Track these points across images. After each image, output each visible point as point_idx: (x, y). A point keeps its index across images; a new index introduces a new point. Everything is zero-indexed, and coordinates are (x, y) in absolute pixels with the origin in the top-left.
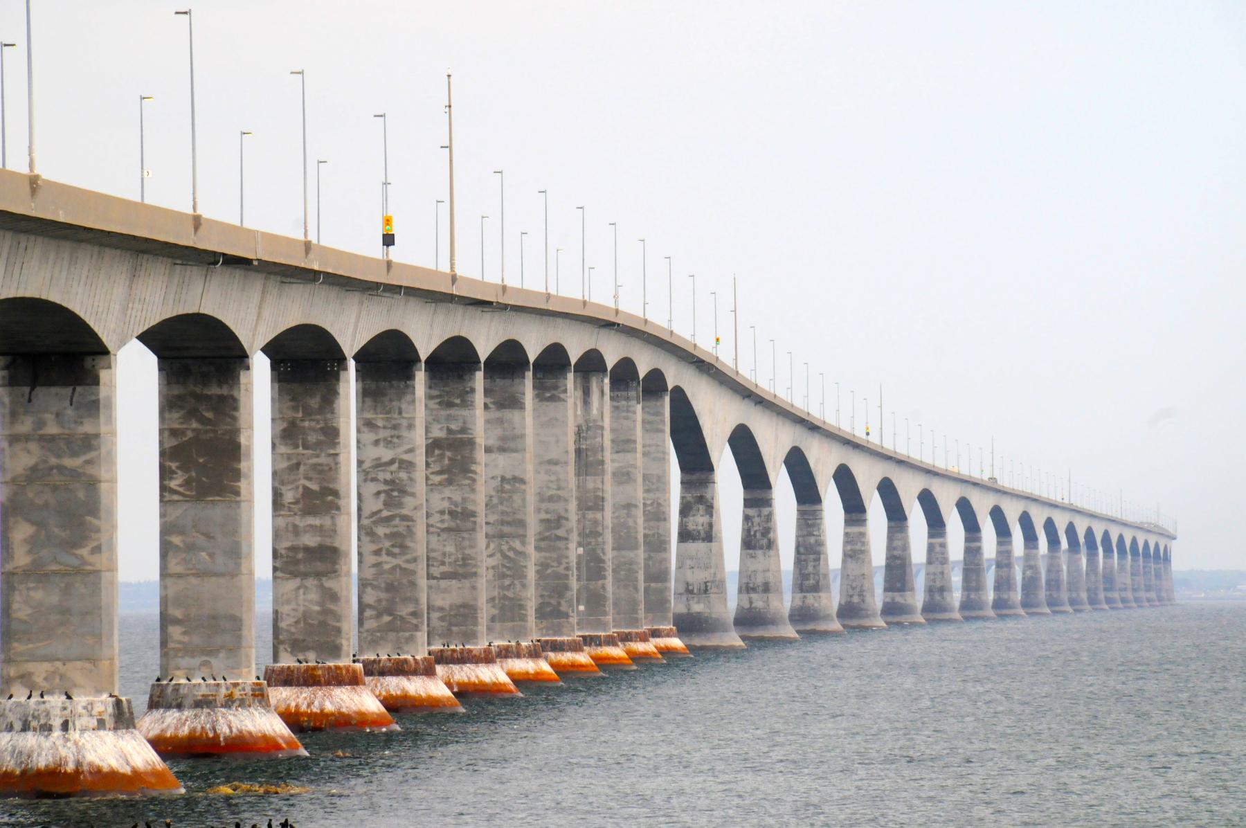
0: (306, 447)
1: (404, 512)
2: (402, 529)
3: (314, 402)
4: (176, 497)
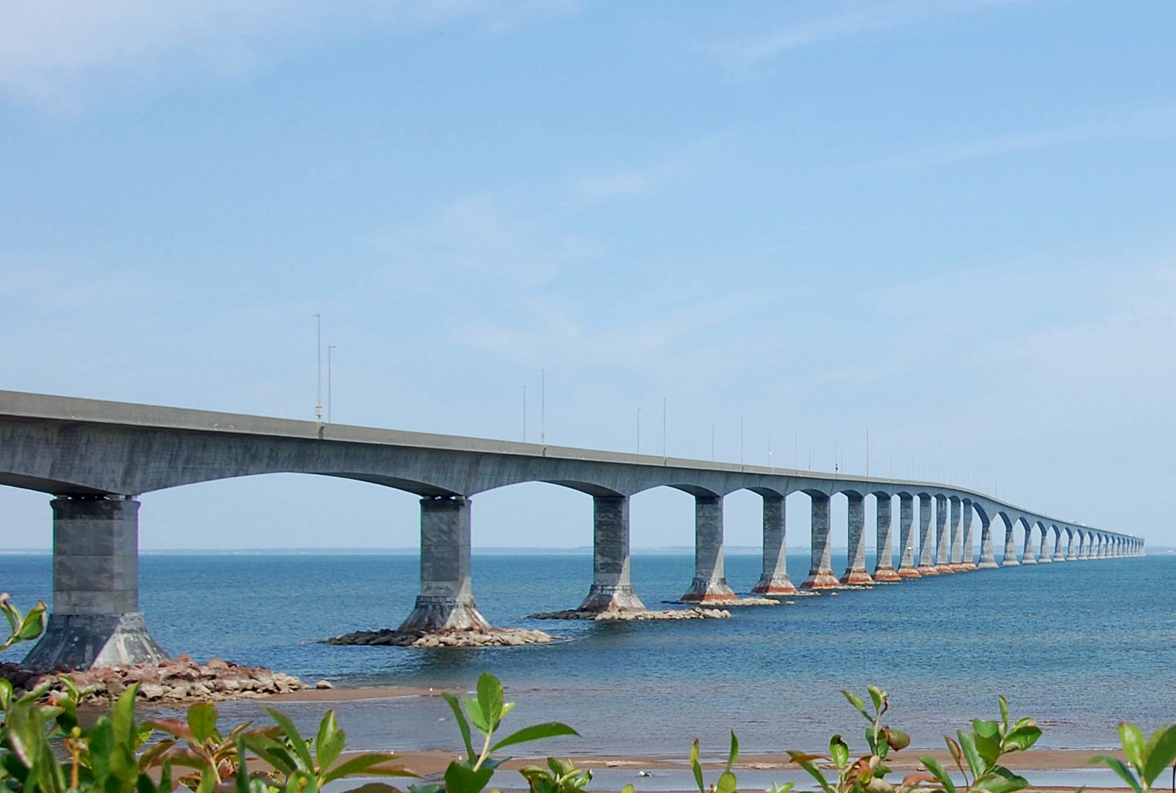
0: (820, 518)
3: (821, 507)
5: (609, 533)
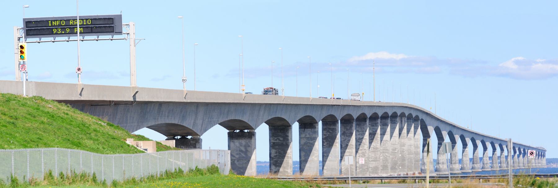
0: (347, 136)
1: (365, 148)
2: (364, 152)
3: (348, 128)
4: (325, 147)
5: (280, 150)
